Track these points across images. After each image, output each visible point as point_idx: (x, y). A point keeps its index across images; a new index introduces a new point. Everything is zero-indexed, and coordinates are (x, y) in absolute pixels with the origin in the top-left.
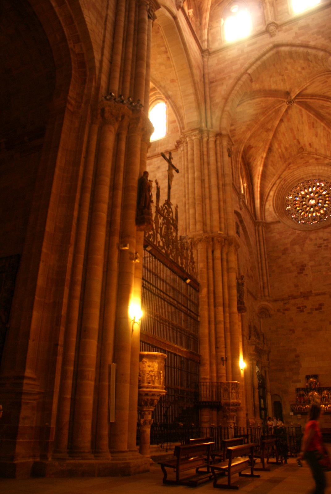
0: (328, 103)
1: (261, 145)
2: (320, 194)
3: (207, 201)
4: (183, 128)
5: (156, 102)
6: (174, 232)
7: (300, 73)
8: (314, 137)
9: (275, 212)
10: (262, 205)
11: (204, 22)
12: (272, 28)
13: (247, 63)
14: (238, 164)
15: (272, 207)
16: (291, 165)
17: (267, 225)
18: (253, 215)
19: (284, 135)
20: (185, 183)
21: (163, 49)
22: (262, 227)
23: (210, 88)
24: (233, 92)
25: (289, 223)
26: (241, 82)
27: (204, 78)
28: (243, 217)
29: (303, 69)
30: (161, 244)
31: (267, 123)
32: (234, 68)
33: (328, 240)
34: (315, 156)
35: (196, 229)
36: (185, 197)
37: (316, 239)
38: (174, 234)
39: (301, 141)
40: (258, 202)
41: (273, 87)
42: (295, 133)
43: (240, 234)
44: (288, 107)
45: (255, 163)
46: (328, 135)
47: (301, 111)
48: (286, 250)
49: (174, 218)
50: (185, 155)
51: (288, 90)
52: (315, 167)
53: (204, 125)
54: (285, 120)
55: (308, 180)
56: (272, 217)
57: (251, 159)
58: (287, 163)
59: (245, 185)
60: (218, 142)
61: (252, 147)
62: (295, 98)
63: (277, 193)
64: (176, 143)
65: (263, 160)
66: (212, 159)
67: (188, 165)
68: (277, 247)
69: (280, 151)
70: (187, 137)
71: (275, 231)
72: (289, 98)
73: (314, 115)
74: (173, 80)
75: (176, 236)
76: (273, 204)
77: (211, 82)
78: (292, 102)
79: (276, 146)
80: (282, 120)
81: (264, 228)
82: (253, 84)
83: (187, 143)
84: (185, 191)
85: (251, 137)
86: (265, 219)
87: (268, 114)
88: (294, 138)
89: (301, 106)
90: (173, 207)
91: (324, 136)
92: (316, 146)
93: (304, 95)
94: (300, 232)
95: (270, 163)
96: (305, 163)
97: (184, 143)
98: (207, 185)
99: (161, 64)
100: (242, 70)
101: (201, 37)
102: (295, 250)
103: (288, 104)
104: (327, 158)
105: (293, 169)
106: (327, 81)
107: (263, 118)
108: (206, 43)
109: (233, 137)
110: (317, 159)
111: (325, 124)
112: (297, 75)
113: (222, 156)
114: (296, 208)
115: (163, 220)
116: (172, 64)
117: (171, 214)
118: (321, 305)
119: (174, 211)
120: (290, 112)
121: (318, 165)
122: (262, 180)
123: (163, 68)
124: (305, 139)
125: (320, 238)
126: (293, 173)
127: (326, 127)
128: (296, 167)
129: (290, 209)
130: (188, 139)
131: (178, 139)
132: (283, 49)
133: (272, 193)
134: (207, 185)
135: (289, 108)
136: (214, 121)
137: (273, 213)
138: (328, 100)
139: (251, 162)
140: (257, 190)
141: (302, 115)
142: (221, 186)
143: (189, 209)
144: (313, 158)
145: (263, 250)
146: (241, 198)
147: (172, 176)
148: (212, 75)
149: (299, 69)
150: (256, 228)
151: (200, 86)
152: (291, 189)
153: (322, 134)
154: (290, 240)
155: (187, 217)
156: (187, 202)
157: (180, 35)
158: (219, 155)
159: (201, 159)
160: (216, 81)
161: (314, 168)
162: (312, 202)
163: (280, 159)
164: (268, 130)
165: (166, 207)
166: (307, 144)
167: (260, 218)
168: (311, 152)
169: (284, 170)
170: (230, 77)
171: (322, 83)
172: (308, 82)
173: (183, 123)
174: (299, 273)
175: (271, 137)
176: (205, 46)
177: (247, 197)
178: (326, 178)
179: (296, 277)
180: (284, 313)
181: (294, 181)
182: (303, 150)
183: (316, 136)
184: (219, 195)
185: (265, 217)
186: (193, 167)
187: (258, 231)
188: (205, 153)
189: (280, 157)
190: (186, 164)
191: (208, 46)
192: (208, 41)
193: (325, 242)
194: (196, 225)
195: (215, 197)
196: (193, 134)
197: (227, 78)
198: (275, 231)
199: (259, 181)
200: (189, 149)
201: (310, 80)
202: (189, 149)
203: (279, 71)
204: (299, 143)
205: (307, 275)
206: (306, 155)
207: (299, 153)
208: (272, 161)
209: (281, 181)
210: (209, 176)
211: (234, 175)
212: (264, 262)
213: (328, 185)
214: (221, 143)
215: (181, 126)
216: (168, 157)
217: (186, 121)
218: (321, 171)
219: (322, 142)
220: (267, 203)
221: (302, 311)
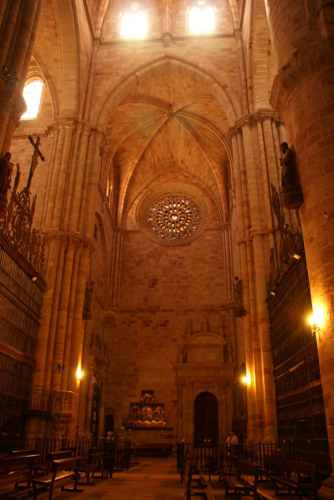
0: (206, 125)
1: (135, 150)
2: (184, 212)
3: (69, 197)
4: (58, 114)
5: (34, 78)
6: (28, 224)
7: (186, 89)
8: (187, 155)
9: (137, 222)
10: (125, 211)
11: (101, 8)
12: (167, 38)
13: (137, 65)
14: (108, 165)
15: (134, 215)
16: (160, 177)
17: (127, 233)
18: (114, 221)
19: (159, 145)
20: (49, 172)
21: (52, 23)
22: (121, 234)
23: (94, 80)
24: (117, 90)
25: (149, 235)
26: (127, 82)
27: (90, 68)
28: (103, 220)
29: (189, 86)
30: (11, 234)
32: (123, 66)
33: (183, 258)
34: (185, 173)
35: (52, 224)
36: (46, 188)
37: (172, 255)
38: (28, 226)
39: (174, 156)
40: (121, 207)
41: (158, 96)
43: (98, 238)
44: (168, 119)
45: (126, 167)
46: (200, 155)
47: (180, 126)
48: (141, 261)
49: (30, 208)
50: (55, 143)
51: (171, 102)
52: (183, 184)
53: (80, 116)
55: (174, 195)
56: (132, 226)
57: (122, 162)
58: (157, 174)
59: (112, 188)
60: (92, 138)
61: (126, 151)
62: (177, 112)
63: (142, 203)
64: (47, 129)
65: (134, 166)
66: (83, 154)
67: (55, 155)
68: (133, 257)
70: (60, 124)
71: (133, 240)
72: (171, 111)
73: (191, 133)
74: (56, 59)
75: (30, 228)
76: (136, 212)
77: (97, 74)
78: (173, 116)
79: (149, 155)
80: (159, 131)
81: (122, 235)
82: (139, 87)
83: (59, 131)
84: (47, 182)
85: (126, 140)
86: (125, 227)
87: (147, 121)
88: (169, 152)
89: (180, 121)
90: (31, 197)
91: (197, 155)
93: (185, 112)
94: (157, 245)
95: (140, 170)
96: (175, 178)
97: (56, 130)
98: (71, 180)
99: (46, 39)
100: (131, 71)
101: (96, 23)
103: (168, 117)
104: (195, 178)
105: (162, 181)
106: (208, 105)
107: (142, 124)
108: (99, 31)
109: (108, 135)
110: (186, 177)
111: (200, 145)
112: (183, 91)
113: (94, 153)
114: (158, 221)
115: (18, 208)
116: (59, 43)
117: (28, 204)
118: (167, 322)
119: (32, 201)
120: (169, 124)
121: (186, 182)
122: (129, 186)
123: (48, 43)
125: (176, 255)
126: (161, 186)
127: (200, 148)
128: (165, 180)
129: (152, 221)
130: (61, 127)
131: (50, 124)
132: (174, 61)
133: (136, 202)
134: (71, 180)
135: (168, 120)
136: (92, 115)
137: (135, 221)
138: (206, 122)
140: (123, 194)
142: (86, 184)
143: (48, 201)
144: (182, 174)
145: (117, 259)
146: (104, 201)
147: (37, 163)
148: (99, 67)
149: (186, 86)
150: (115, 234)
151: (85, 74)
152: (156, 201)
153: (195, 154)
154: (147, 252)
155: (45, 210)
156: (47, 194)
157: (74, 14)
158: (90, 151)
159: (70, 151)
160: (102, 74)
161: (182, 185)
162: (175, 218)
163: (150, 169)
164: (144, 137)
165: (23, 195)
166: (180, 160)
167: (120, 224)
168: (182, 169)
169: (153, 181)
170: (117, 74)
171: (204, 106)
172: (191, 100)
173: (58, 109)
174: (150, 287)
175: (146, 145)
176: (98, 34)
177: (111, 202)
178: (191, 198)
179: (147, 290)
180: (129, 326)
181: (161, 194)
182: (175, 165)
183: (190, 154)
184: (82, 193)
185: (125, 224)
186: (61, 158)
187: (116, 237)
188: (76, 146)
189: (152, 168)
190: (53, 153)
191: (101, 35)
192: (102, 30)
193: (180, 260)
194: (52, 220)
195: (78, 195)
196: (67, 122)
197: (114, 74)
198: (133, 240)
199: (126, 186)
200: (60, 138)
201: (193, 99)
202: (60, 138)
203: (166, 82)
204: (172, 157)
205: (158, 289)
206: (177, 170)
207: (170, 167)
208: (142, 169)
209: (148, 191)
210: (76, 171)
211: (102, 176)
212: (117, 270)
213: (192, 204)
214: (95, 139)
215: (56, 112)
216: (35, 142)
217: (62, 107)
218: (188, 190)
219: (194, 161)
220: (131, 211)
221: (147, 325)
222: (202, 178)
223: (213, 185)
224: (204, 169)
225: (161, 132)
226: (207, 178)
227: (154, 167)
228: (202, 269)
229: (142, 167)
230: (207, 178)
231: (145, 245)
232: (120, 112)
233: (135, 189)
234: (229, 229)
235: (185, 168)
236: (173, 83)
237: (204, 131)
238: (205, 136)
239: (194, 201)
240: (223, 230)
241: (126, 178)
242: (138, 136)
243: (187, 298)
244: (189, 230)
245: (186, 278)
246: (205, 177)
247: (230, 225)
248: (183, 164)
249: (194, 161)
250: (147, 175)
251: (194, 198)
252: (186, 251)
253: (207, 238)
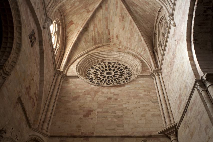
8: (121, 30)
9: (77, 71)
16: (99, 48)
19: (100, 21)
31: (90, 5)
37: (107, 93)
39: (111, 33)
42: (109, 23)
46: (132, 29)
47: (117, 3)
54: (104, 7)
58: (96, 46)
61: (73, 23)
65: (79, 33)
69: (94, 33)
71: (72, 83)
79: (91, 28)
80: (100, 7)
91: (129, 29)
92: (121, 38)
95: (83, 39)
102: (86, 98)
110: (119, 49)
122: (73, 47)
124: (115, 29)
139: (68, 36)
141: (117, 7)
144: (116, 47)
181: (99, 60)
182: (111, 41)
183: (123, 29)
198: (72, 83)
199: (71, 47)
208: (85, 39)
209: (88, 55)
219: (126, 35)
222: (132, 48)
223: (142, 51)
224: (135, 40)
225: (102, 8)
226: (137, 46)
227: (94, 39)
228: (137, 103)
229: (85, 36)
230: (137, 46)
231: (83, 86)
233: (78, 53)
234: (160, 74)
235: (119, 43)
238: (137, 12)
239: (126, 65)
240: (153, 76)
241: (72, 42)
242: (84, 10)
243: (123, 126)
244: (122, 81)
245: (122, 110)
246: (135, 46)
247: (160, 70)
248: (117, 39)
249: (126, 35)
250: (89, 45)
251: (126, 63)
252: (121, 91)
253: (140, 82)
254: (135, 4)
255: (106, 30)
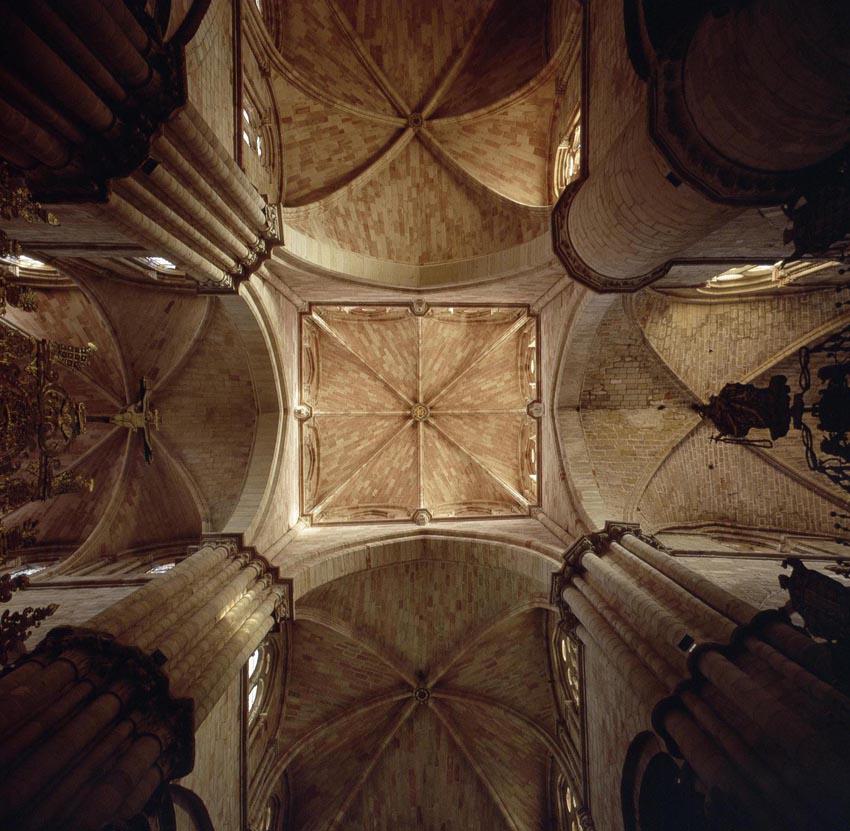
7: (453, 618)
19: (394, 783)
21: (244, 450)
29: (459, 606)
80: (396, 742)
141: (438, 740)
171: (488, 667)
183: (461, 805)
225: (399, 746)
232: (324, 675)
236: (431, 606)
237: (490, 739)
254: (485, 730)
255: (413, 808)
